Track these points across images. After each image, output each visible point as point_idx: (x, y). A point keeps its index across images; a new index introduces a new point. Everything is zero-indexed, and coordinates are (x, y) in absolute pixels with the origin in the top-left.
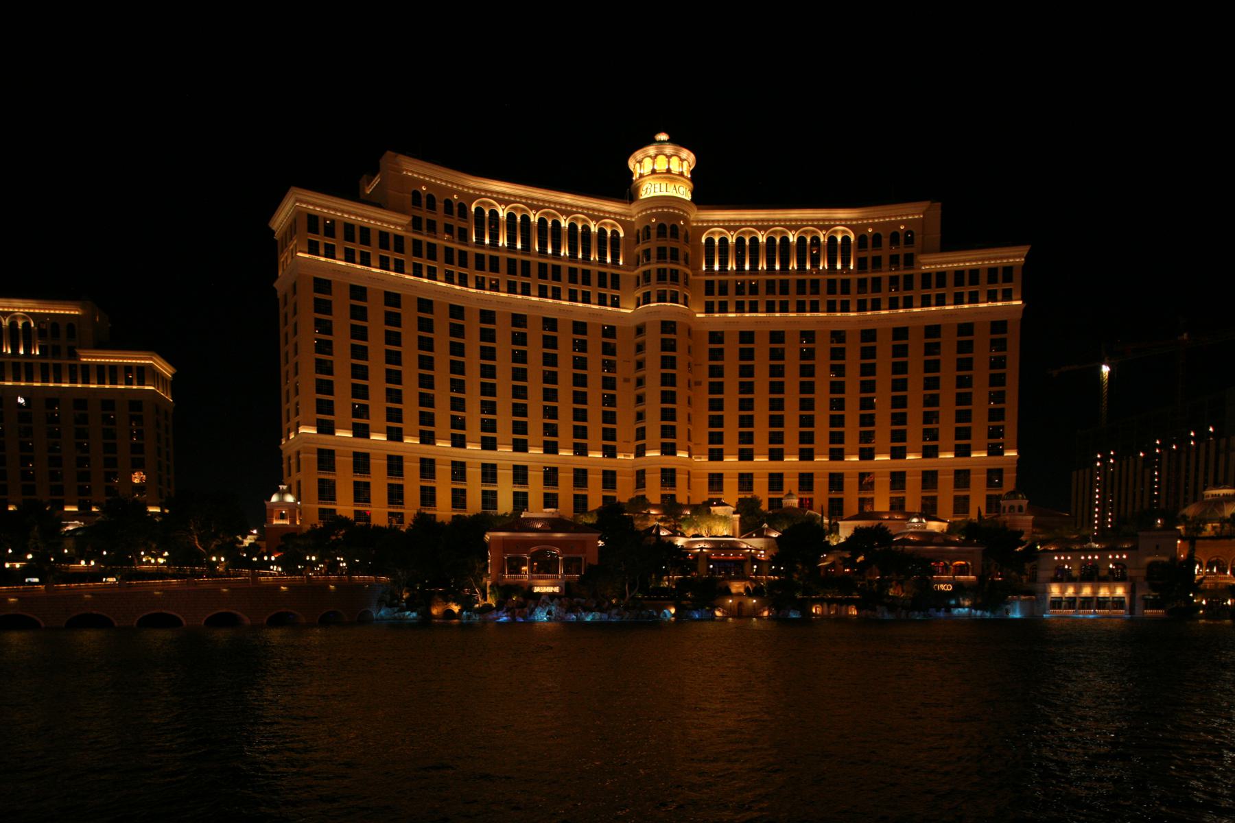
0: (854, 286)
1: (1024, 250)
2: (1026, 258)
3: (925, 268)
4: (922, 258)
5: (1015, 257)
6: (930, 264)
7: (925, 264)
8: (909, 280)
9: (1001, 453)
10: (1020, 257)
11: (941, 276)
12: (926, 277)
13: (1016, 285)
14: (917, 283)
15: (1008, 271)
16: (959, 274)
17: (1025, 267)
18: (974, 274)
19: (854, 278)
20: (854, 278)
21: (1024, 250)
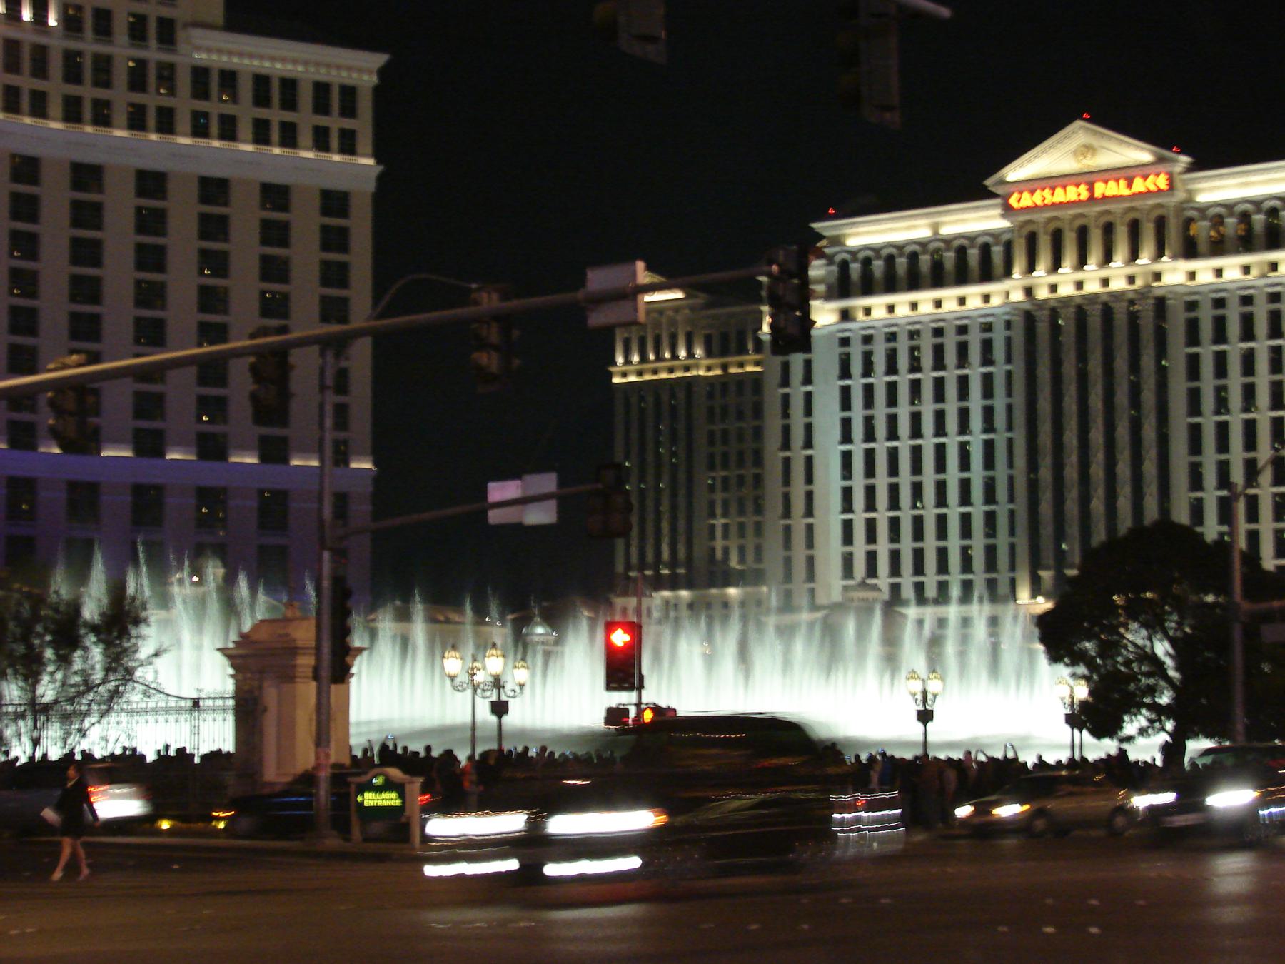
0: (56, 66)
1: (379, 59)
2: (382, 72)
3: (200, 57)
4: (197, 35)
5: (359, 68)
6: (209, 50)
7: (199, 49)
8: (167, 75)
9: (222, 455)
10: (370, 72)
11: (229, 78)
12: (200, 75)
13: (363, 125)
14: (184, 82)
15: (349, 93)
16: (262, 81)
17: (377, 91)
18: (289, 85)
19: (57, 46)
20: (57, 46)
21: (380, 59)
